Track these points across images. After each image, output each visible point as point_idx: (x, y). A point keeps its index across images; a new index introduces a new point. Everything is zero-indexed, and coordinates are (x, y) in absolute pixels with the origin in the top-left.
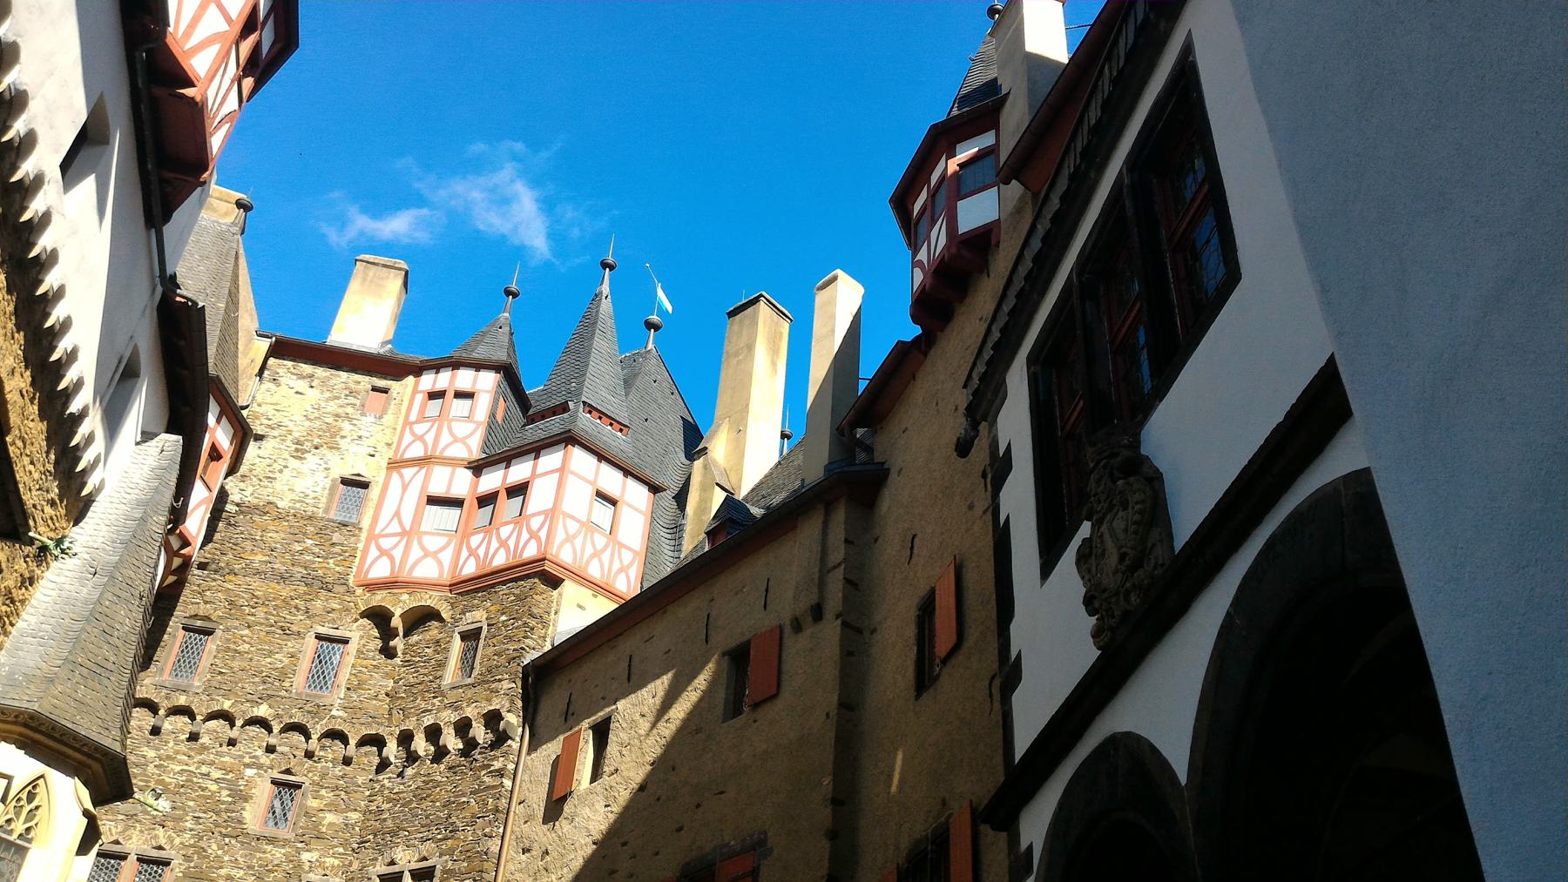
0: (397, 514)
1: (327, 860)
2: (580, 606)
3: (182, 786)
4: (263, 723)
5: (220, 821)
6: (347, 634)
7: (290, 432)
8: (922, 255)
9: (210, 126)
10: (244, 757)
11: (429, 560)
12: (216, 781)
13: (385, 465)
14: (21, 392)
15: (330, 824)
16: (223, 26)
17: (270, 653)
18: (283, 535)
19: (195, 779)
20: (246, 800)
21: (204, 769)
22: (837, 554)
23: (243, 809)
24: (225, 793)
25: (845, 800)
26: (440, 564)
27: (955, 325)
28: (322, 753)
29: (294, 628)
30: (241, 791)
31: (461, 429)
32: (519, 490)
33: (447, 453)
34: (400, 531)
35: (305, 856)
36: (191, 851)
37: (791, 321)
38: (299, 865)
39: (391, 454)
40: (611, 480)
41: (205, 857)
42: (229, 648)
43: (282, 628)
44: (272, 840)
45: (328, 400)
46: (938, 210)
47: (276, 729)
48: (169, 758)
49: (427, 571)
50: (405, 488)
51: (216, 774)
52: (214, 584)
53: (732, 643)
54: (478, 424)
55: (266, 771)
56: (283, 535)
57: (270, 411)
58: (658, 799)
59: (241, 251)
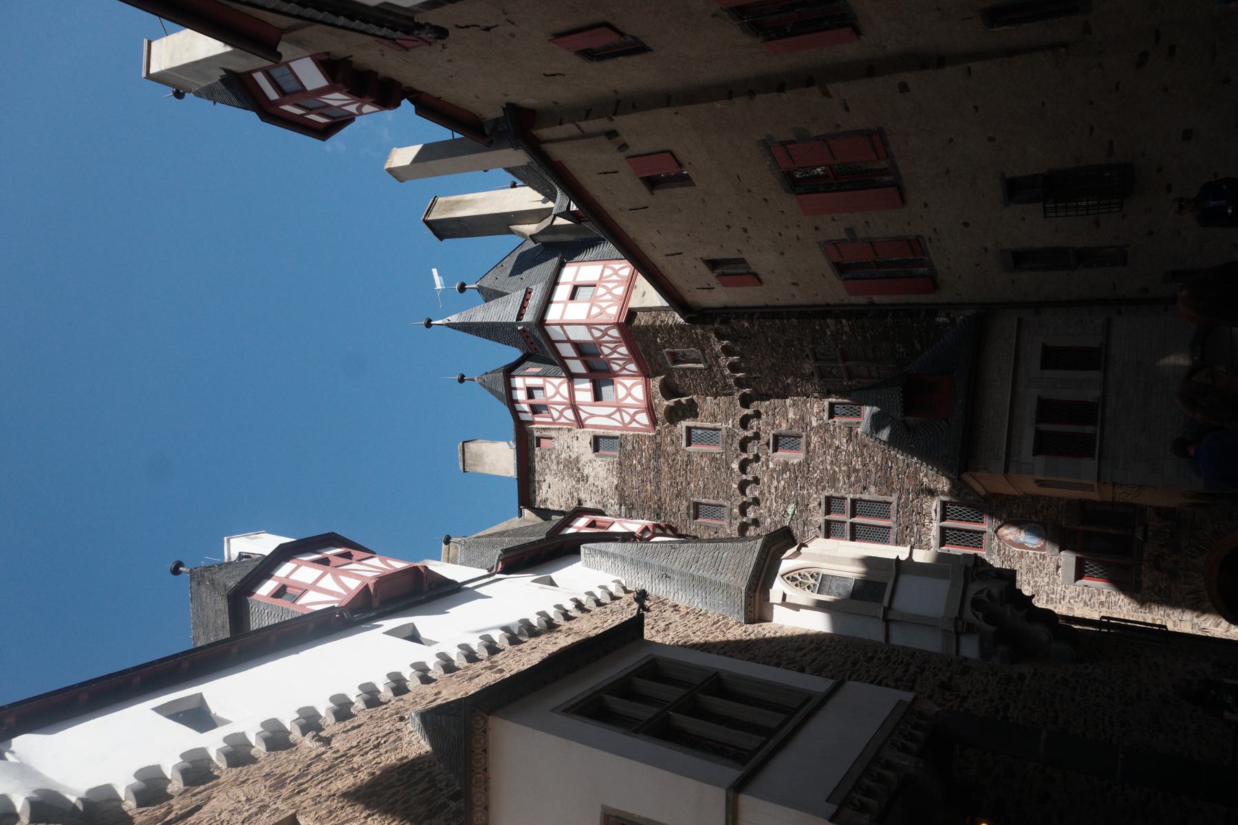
0: (609, 416)
1: (815, 411)
2: (644, 295)
3: (784, 500)
5: (800, 475)
6: (684, 429)
7: (573, 486)
8: (352, 108)
9: (389, 570)
10: (763, 471)
11: (633, 392)
12: (778, 482)
13: (582, 430)
14: (566, 636)
15: (794, 414)
16: (329, 577)
18: (634, 477)
20: (788, 463)
21: (773, 490)
22: (570, 129)
23: (792, 464)
24: (785, 476)
25: (729, 91)
26: (633, 385)
27: (393, 75)
28: (755, 428)
29: (686, 459)
31: (550, 390)
32: (577, 346)
33: (566, 394)
34: (618, 413)
35: (814, 424)
36: (819, 487)
37: (436, 197)
38: (820, 426)
39: (574, 428)
40: (562, 292)
41: (822, 479)
42: (703, 492)
43: (687, 465)
44: (808, 444)
45: (550, 470)
46: (318, 104)
47: (745, 456)
48: (769, 511)
49: (639, 392)
50: (593, 415)
51: (775, 483)
52: (668, 508)
53: (643, 189)
54: (545, 381)
55: (770, 456)
56: (634, 477)
57: (562, 501)
58: (750, 218)
59: (475, 536)
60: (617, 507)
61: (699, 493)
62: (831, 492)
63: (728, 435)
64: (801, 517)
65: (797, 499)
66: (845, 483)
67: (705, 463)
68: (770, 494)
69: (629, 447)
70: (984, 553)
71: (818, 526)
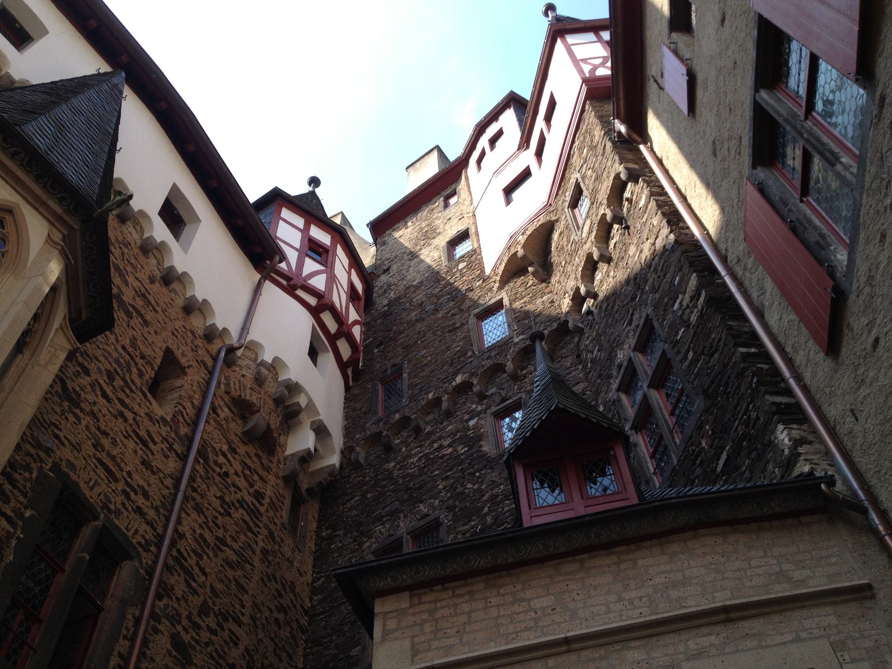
3: (424, 467)
4: (465, 387)
12: (449, 446)
17: (448, 348)
19: (432, 456)
20: (480, 440)
21: (436, 445)
23: (481, 446)
24: (459, 448)
29: (458, 325)
30: (472, 437)
36: (451, 502)
51: (446, 443)
55: (485, 413)
57: (388, 256)
60: (386, 302)
62: (446, 519)
63: (501, 346)
65: (429, 482)
66: (464, 534)
67: (458, 346)
68: (429, 445)
69: (461, 266)
71: (391, 532)
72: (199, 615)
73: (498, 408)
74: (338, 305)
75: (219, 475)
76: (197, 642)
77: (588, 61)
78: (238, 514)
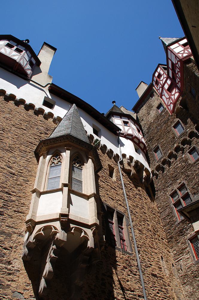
3: (175, 171)
6: (177, 120)
7: (145, 114)
12: (179, 164)
43: (167, 133)
47: (180, 145)
60: (146, 129)
61: (162, 144)
62: (186, 183)
64: (172, 181)
70: (196, 260)
72: (140, 222)
73: (189, 150)
74: (137, 136)
75: (130, 189)
76: (142, 228)
77: (180, 53)
78: (137, 196)
